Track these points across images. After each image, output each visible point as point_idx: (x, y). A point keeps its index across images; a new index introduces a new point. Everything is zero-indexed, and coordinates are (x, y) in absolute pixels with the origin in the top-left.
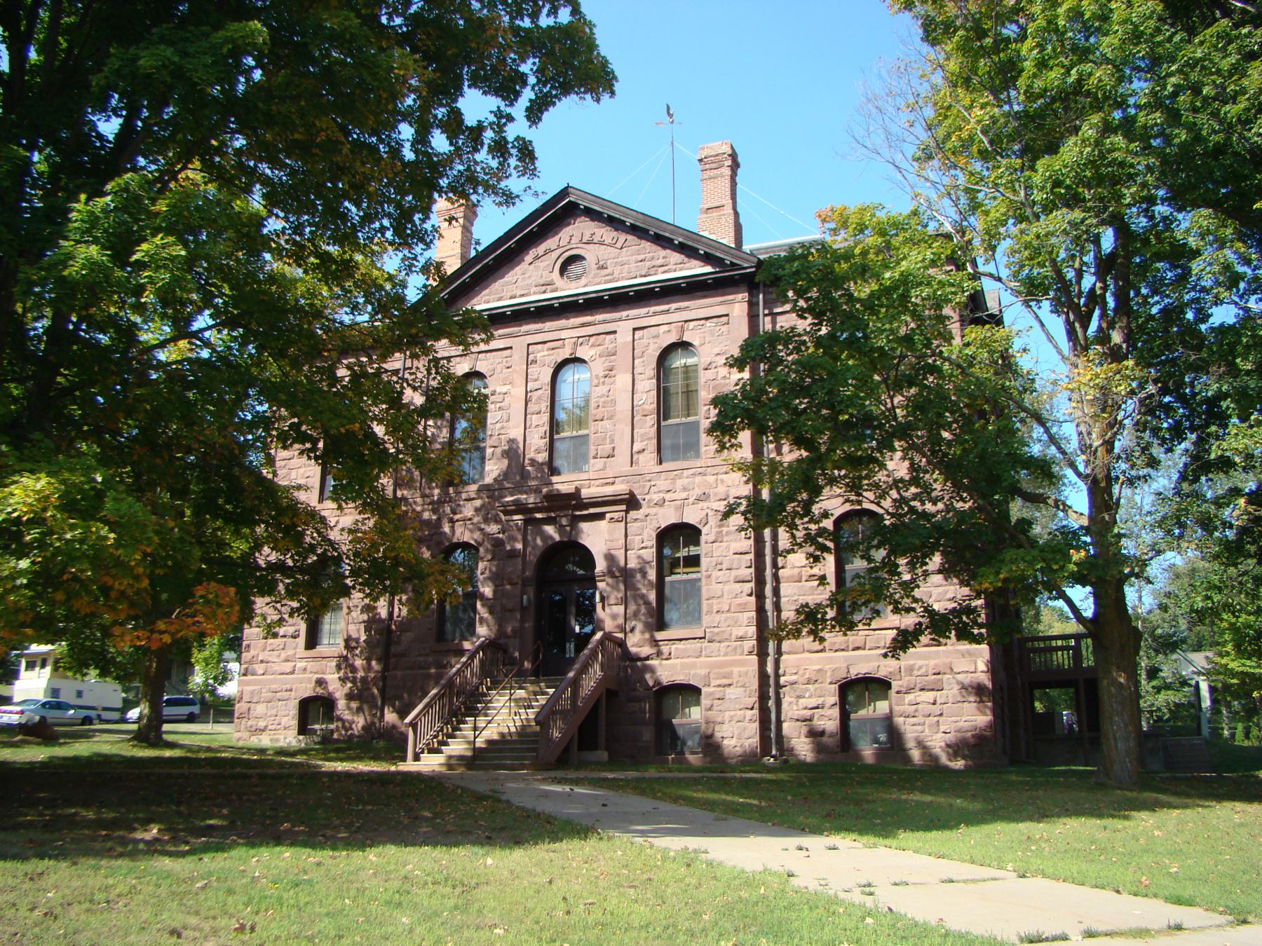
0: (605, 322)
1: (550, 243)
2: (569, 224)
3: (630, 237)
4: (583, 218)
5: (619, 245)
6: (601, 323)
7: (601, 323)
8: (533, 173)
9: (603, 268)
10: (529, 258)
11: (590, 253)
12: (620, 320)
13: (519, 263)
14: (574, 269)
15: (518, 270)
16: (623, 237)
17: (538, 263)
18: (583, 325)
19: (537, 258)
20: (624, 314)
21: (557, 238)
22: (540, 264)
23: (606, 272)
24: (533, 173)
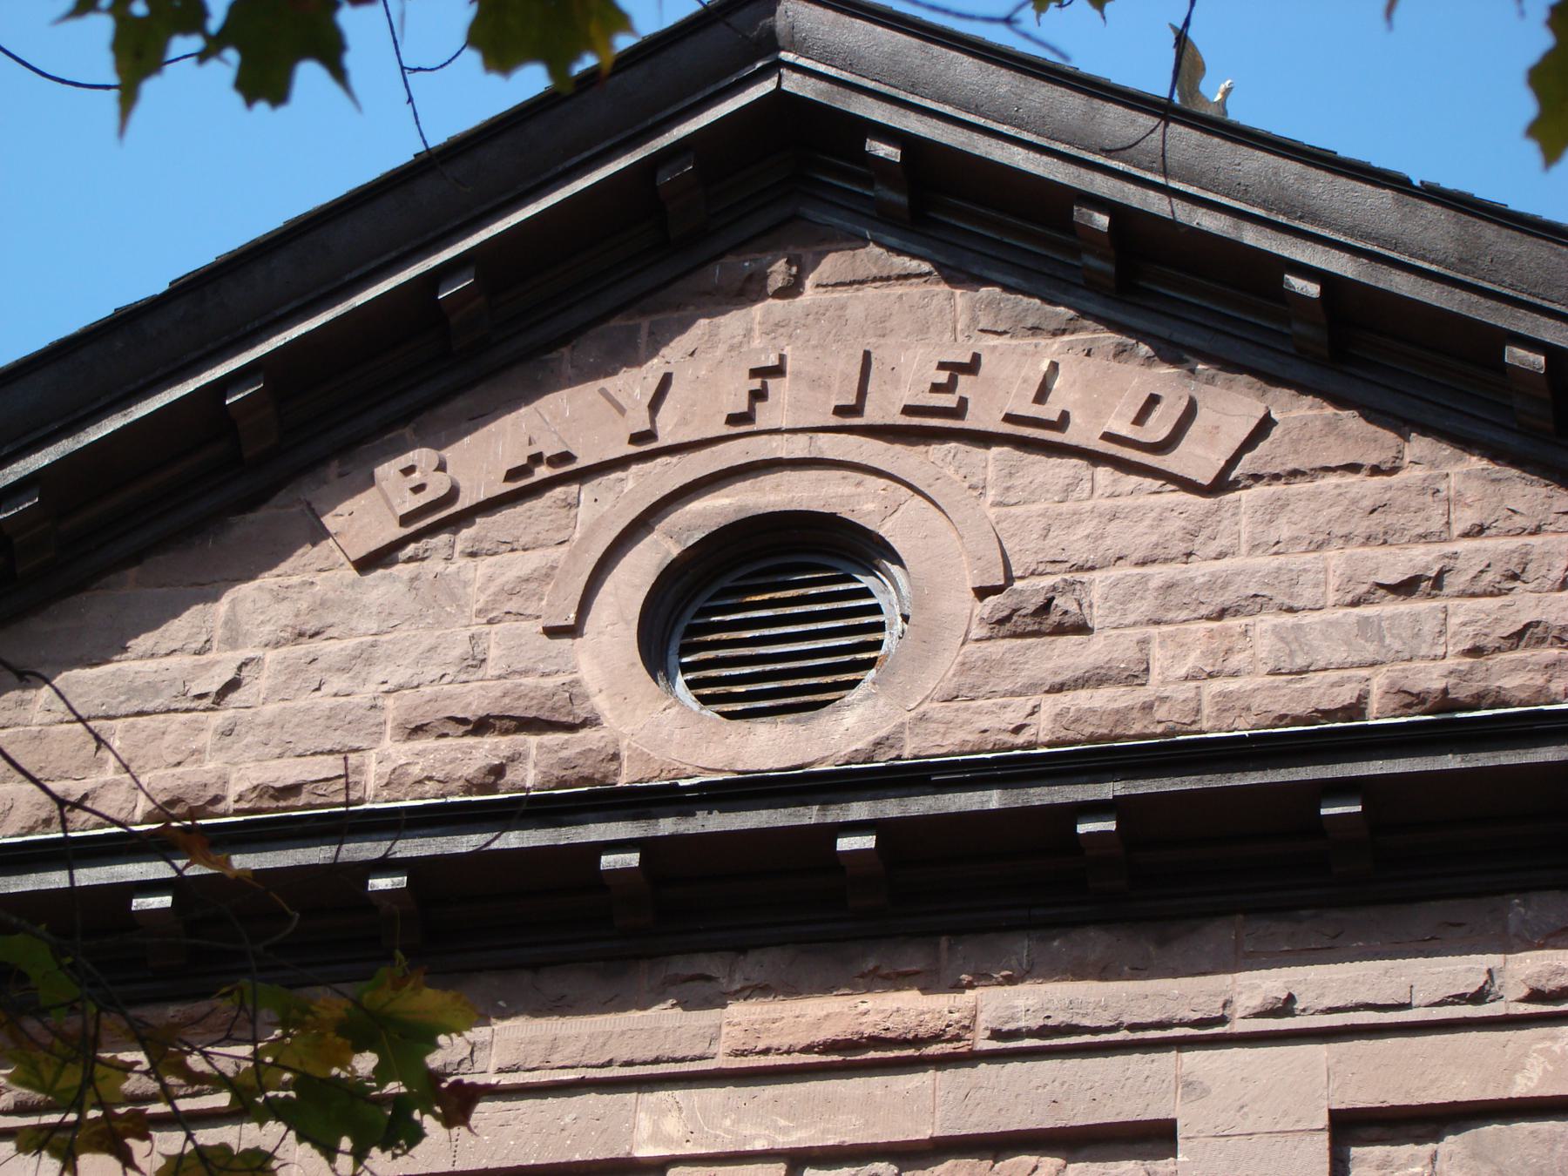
0: (1057, 1042)
1: (573, 416)
2: (748, 291)
3: (1298, 413)
4: (872, 257)
5: (1199, 457)
6: (1012, 1047)
7: (1012, 1047)
8: (1206, 1092)
9: (1048, 621)
10: (365, 516)
11: (941, 531)
12: (1210, 1035)
13: (270, 554)
14: (768, 625)
15: (255, 606)
16: (1229, 407)
17: (442, 558)
18: (849, 1058)
19: (443, 517)
20: (1249, 990)
21: (633, 384)
22: (464, 570)
23: (1067, 655)
24: (1206, 1092)
